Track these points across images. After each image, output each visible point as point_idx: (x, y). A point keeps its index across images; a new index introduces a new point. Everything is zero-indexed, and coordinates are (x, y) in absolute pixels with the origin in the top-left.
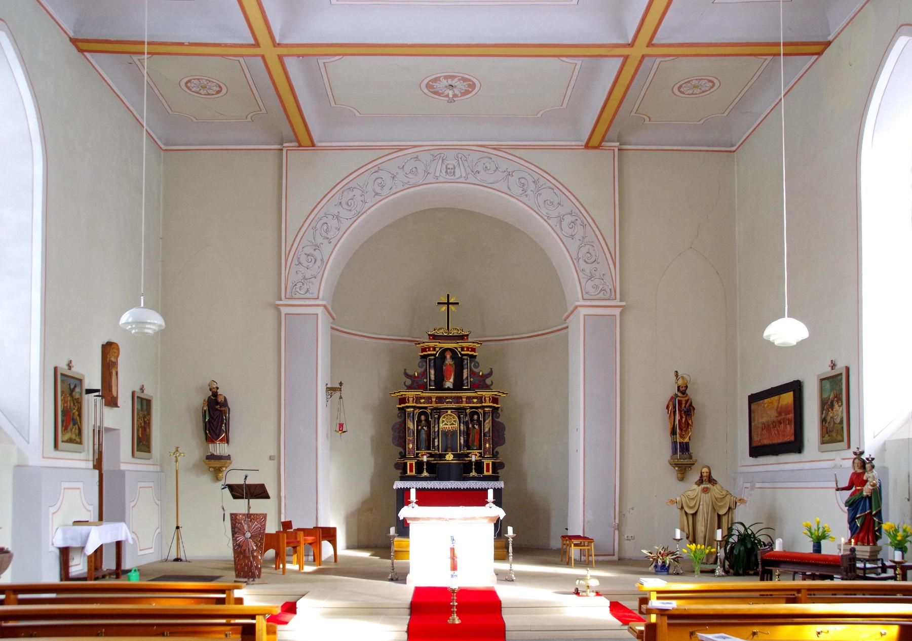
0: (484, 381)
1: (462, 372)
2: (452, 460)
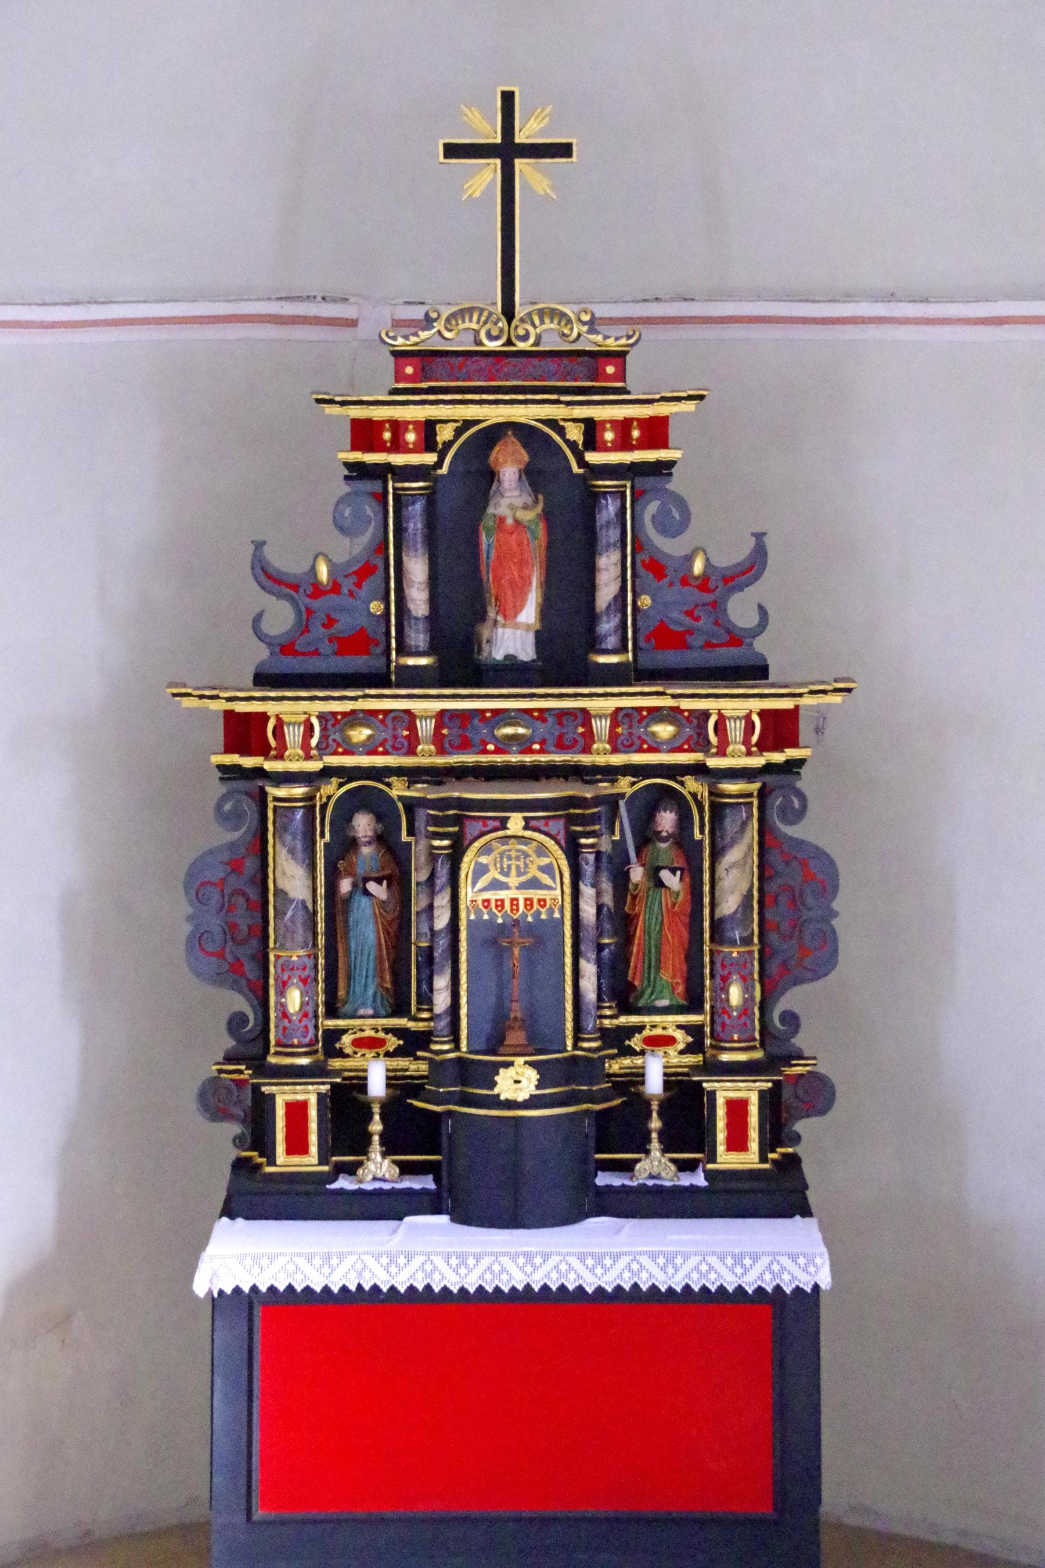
0: (717, 607)
1: (591, 570)
2: (532, 1103)
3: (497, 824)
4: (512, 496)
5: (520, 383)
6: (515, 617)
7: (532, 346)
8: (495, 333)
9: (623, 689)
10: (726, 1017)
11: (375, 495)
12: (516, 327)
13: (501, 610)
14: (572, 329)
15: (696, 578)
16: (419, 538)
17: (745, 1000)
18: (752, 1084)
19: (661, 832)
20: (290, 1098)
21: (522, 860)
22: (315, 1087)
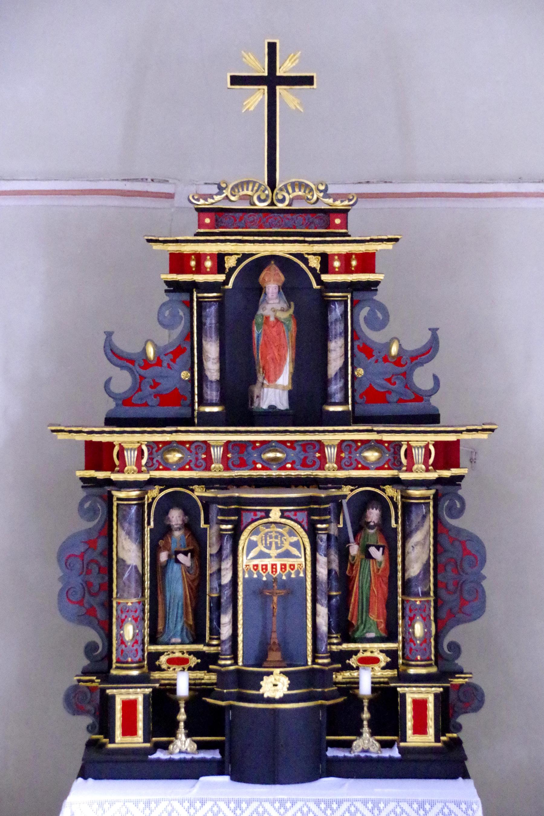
2: (285, 699)
3: (263, 514)
4: (274, 303)
5: (280, 230)
6: (276, 381)
7: (287, 206)
8: (263, 197)
9: (345, 428)
10: (412, 645)
11: (184, 302)
12: (277, 194)
13: (267, 376)
14: (313, 195)
15: (394, 357)
16: (213, 330)
17: (425, 633)
18: (429, 689)
19: (370, 522)
20: (126, 697)
21: (279, 538)
22: (142, 690)
